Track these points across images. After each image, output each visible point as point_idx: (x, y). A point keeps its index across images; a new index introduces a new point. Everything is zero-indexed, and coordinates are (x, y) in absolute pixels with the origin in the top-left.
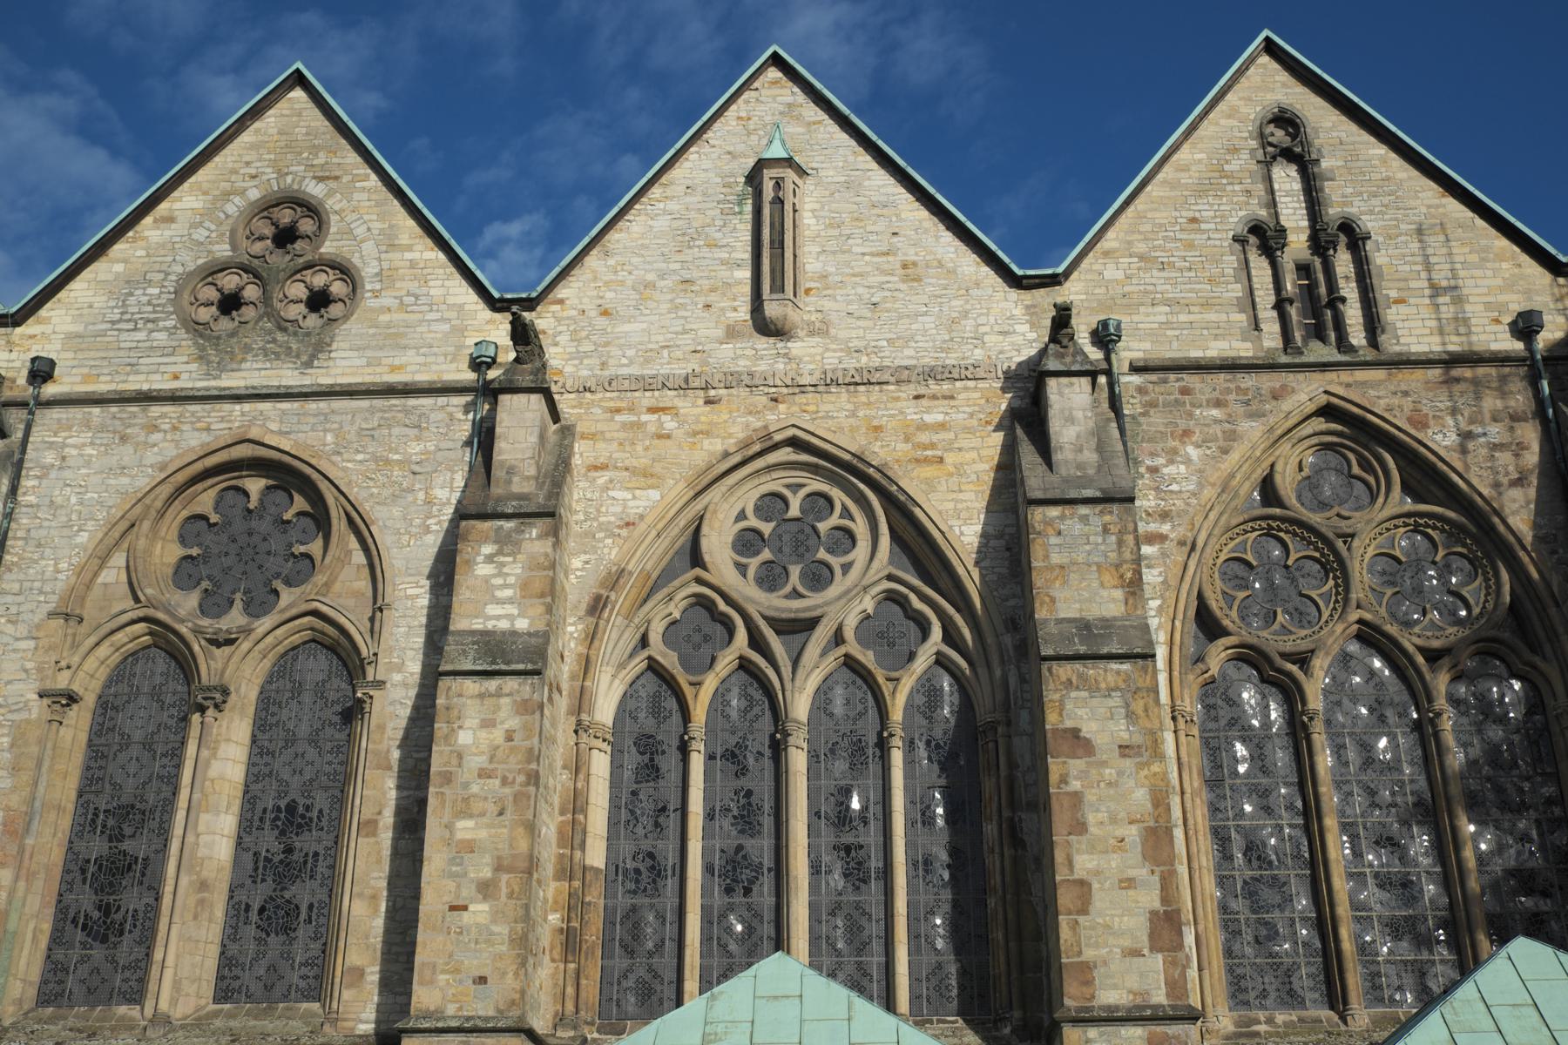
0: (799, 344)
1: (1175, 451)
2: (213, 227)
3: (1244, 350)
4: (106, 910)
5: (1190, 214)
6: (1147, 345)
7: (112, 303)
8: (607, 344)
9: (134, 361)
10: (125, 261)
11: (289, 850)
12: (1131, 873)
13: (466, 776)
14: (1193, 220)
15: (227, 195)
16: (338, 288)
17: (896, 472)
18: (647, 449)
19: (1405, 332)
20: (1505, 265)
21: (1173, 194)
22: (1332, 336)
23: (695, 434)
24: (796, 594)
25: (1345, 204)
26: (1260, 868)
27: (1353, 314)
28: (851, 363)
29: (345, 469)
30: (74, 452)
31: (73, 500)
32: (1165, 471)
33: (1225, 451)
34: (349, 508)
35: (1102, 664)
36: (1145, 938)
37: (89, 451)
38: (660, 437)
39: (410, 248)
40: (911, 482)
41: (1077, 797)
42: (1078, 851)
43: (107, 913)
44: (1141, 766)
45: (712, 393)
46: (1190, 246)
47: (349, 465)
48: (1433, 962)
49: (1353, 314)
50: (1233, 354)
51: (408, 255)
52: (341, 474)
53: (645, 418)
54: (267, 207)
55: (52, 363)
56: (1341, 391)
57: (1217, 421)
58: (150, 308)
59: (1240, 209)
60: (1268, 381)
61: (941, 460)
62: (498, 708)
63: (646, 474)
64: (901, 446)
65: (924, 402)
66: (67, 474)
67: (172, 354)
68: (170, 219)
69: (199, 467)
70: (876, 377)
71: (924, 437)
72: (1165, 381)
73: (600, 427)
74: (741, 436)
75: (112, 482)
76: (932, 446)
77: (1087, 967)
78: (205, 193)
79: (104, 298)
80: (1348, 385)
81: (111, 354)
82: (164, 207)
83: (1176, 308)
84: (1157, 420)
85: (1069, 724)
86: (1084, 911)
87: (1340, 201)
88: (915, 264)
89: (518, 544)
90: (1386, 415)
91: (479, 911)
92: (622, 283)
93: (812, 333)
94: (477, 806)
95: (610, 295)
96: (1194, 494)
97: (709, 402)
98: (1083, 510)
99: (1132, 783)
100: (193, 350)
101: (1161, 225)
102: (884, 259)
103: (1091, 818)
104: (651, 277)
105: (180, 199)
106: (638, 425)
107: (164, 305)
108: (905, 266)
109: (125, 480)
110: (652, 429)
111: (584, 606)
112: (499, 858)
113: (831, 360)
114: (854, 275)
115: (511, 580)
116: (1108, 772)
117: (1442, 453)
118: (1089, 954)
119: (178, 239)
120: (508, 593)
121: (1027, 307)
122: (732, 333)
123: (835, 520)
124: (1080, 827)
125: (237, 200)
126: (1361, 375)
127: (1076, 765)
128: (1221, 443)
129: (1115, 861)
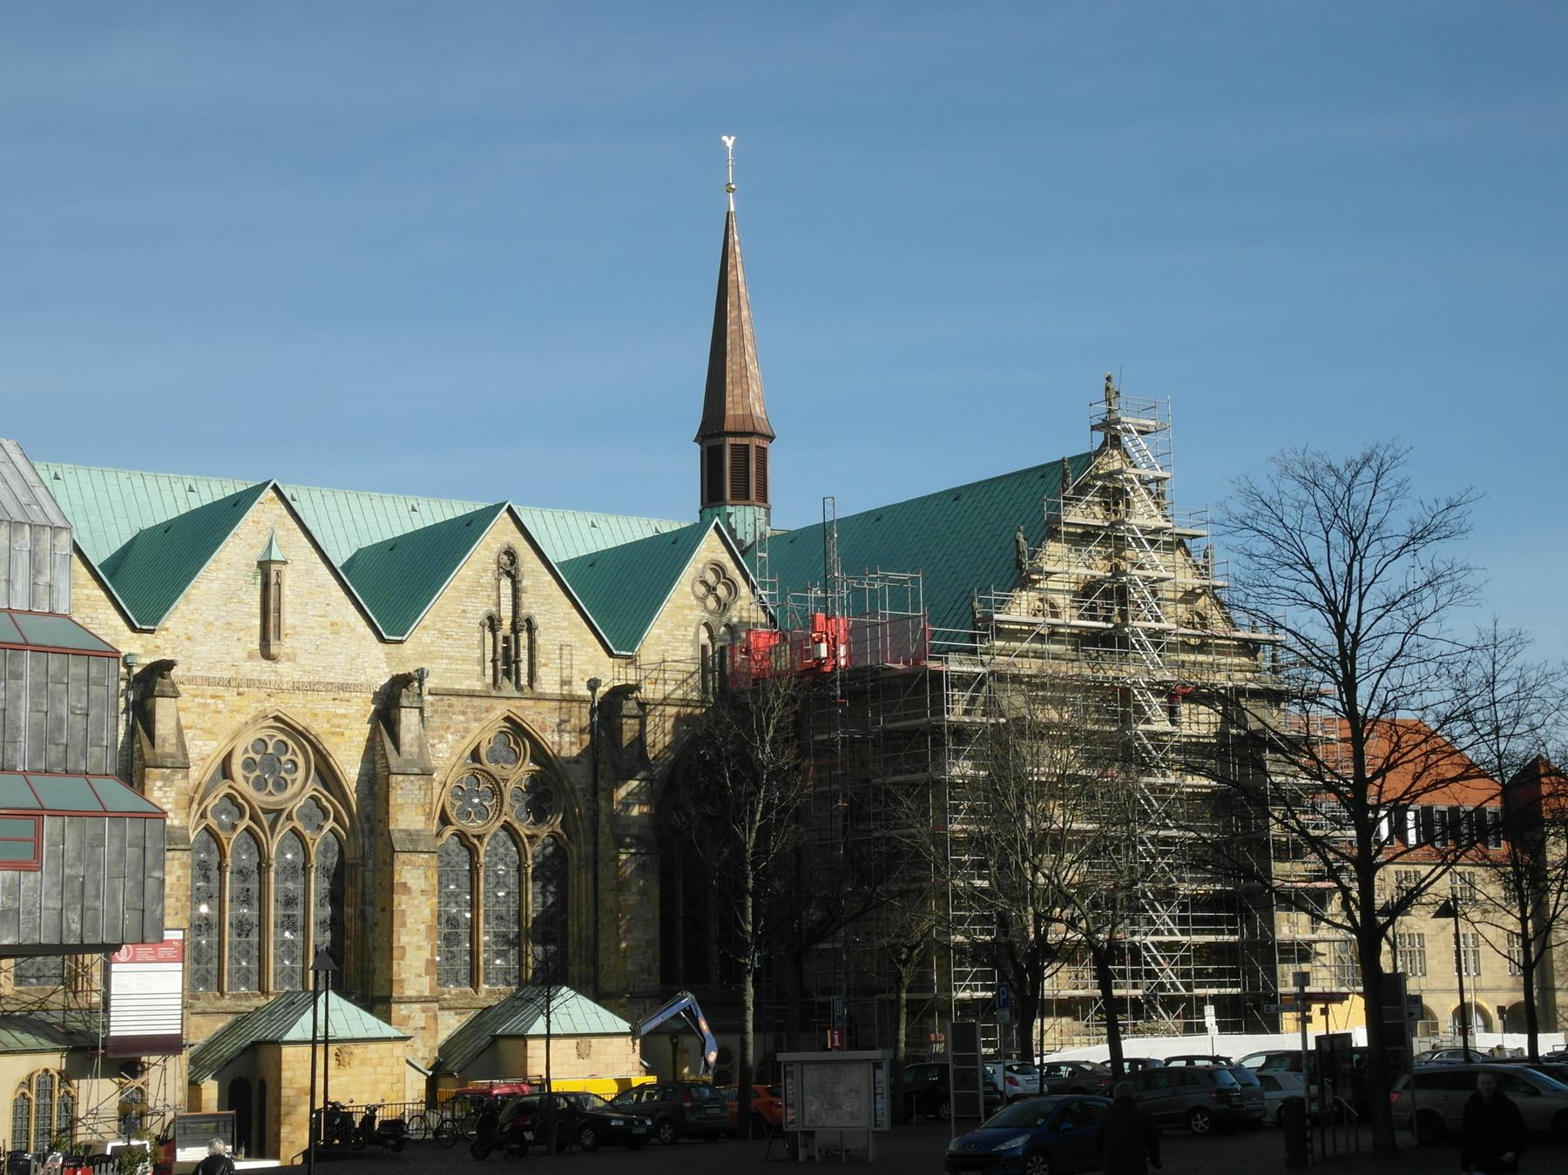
0: (282, 666)
1: (443, 737)
3: (477, 686)
5: (463, 608)
6: (436, 681)
8: (190, 657)
12: (421, 944)
14: (464, 611)
17: (323, 738)
20: (591, 650)
21: (456, 595)
22: (514, 678)
23: (232, 711)
24: (270, 793)
27: (524, 667)
28: (305, 679)
33: (463, 738)
35: (417, 854)
38: (216, 712)
39: (85, 587)
44: (428, 899)
45: (241, 689)
46: (461, 626)
49: (524, 667)
50: (472, 688)
51: (85, 591)
53: (210, 701)
56: (514, 710)
57: (462, 722)
59: (483, 608)
60: (485, 703)
61: (343, 734)
63: (210, 732)
64: (325, 725)
65: (337, 702)
71: (336, 721)
72: (442, 700)
73: (189, 705)
74: (254, 714)
76: (339, 726)
77: (402, 981)
80: (518, 708)
85: (403, 881)
86: (402, 959)
87: (529, 606)
89: (172, 781)
92: (196, 621)
93: (288, 660)
95: (191, 628)
96: (448, 759)
97: (239, 694)
98: (412, 778)
101: (449, 613)
102: (321, 619)
103: (408, 921)
104: (211, 619)
106: (206, 705)
108: (332, 625)
110: (212, 707)
113: (297, 676)
115: (170, 800)
116: (416, 902)
118: (403, 976)
121: (386, 654)
122: (250, 656)
123: (289, 756)
124: (404, 925)
126: (524, 703)
127: (404, 898)
129: (415, 939)
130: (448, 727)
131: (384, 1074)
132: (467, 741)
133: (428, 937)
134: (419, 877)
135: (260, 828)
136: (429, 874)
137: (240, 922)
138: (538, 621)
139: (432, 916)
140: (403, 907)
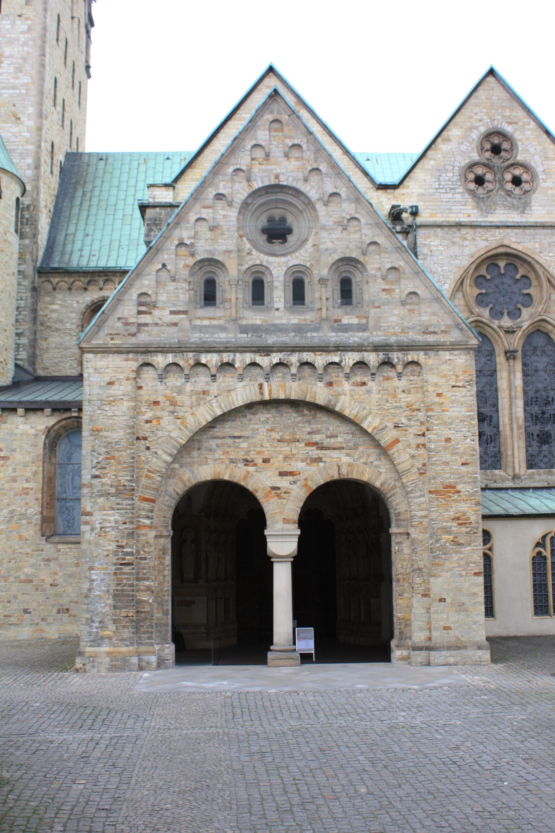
2: (468, 145)
7: (434, 180)
9: (450, 207)
10: (435, 160)
11: (543, 413)
15: (471, 129)
16: (525, 177)
29: (546, 260)
30: (435, 249)
31: (439, 270)
34: (549, 277)
37: (441, 248)
47: (547, 258)
52: (545, 262)
54: (488, 136)
55: (416, 207)
58: (450, 183)
66: (434, 258)
67: (465, 205)
68: (449, 140)
69: (485, 256)
75: (453, 262)
78: (461, 128)
79: (430, 177)
81: (439, 204)
82: (445, 133)
100: (474, 204)
105: (450, 130)
107: (456, 182)
109: (457, 262)
119: (454, 150)
125: (475, 131)
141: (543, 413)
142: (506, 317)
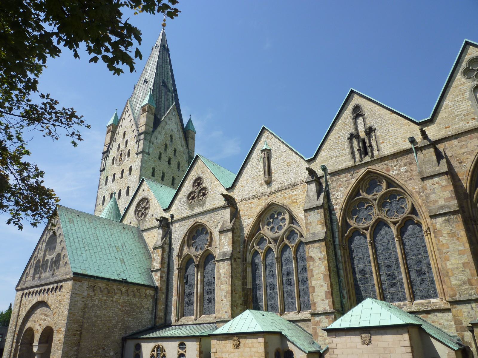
4: (190, 301)
5: (338, 136)
12: (322, 284)
13: (221, 278)
14: (339, 137)
17: (289, 206)
18: (250, 211)
19: (384, 150)
22: (370, 154)
25: (370, 123)
26: (362, 275)
32: (336, 194)
33: (347, 187)
36: (325, 297)
40: (291, 208)
41: (312, 270)
42: (313, 281)
43: (190, 302)
44: (323, 262)
48: (399, 292)
51: (214, 183)
53: (249, 205)
57: (346, 181)
62: (225, 265)
64: (289, 201)
66: (176, 232)
70: (285, 188)
71: (293, 198)
76: (294, 199)
77: (315, 304)
83: (336, 158)
84: (334, 184)
85: (310, 255)
86: (314, 292)
88: (289, 162)
90: (380, 170)
91: (225, 300)
94: (223, 282)
95: (242, 183)
99: (321, 266)
103: (314, 274)
104: (248, 177)
108: (288, 163)
109: (183, 232)
110: (250, 207)
111: (243, 242)
112: (227, 291)
114: (279, 168)
116: (317, 264)
117: (393, 176)
118: (315, 301)
120: (227, 244)
122: (261, 185)
124: (313, 276)
127: (311, 263)
128: (347, 186)
129: (319, 282)
130: (340, 185)
131: (255, 352)
132: (350, 188)
133: (325, 280)
134: (317, 252)
135: (184, 242)
136: (322, 250)
137: (271, 285)
138: (375, 126)
139: (326, 270)
140: (311, 267)
141: (210, 289)
142: (200, 250)
